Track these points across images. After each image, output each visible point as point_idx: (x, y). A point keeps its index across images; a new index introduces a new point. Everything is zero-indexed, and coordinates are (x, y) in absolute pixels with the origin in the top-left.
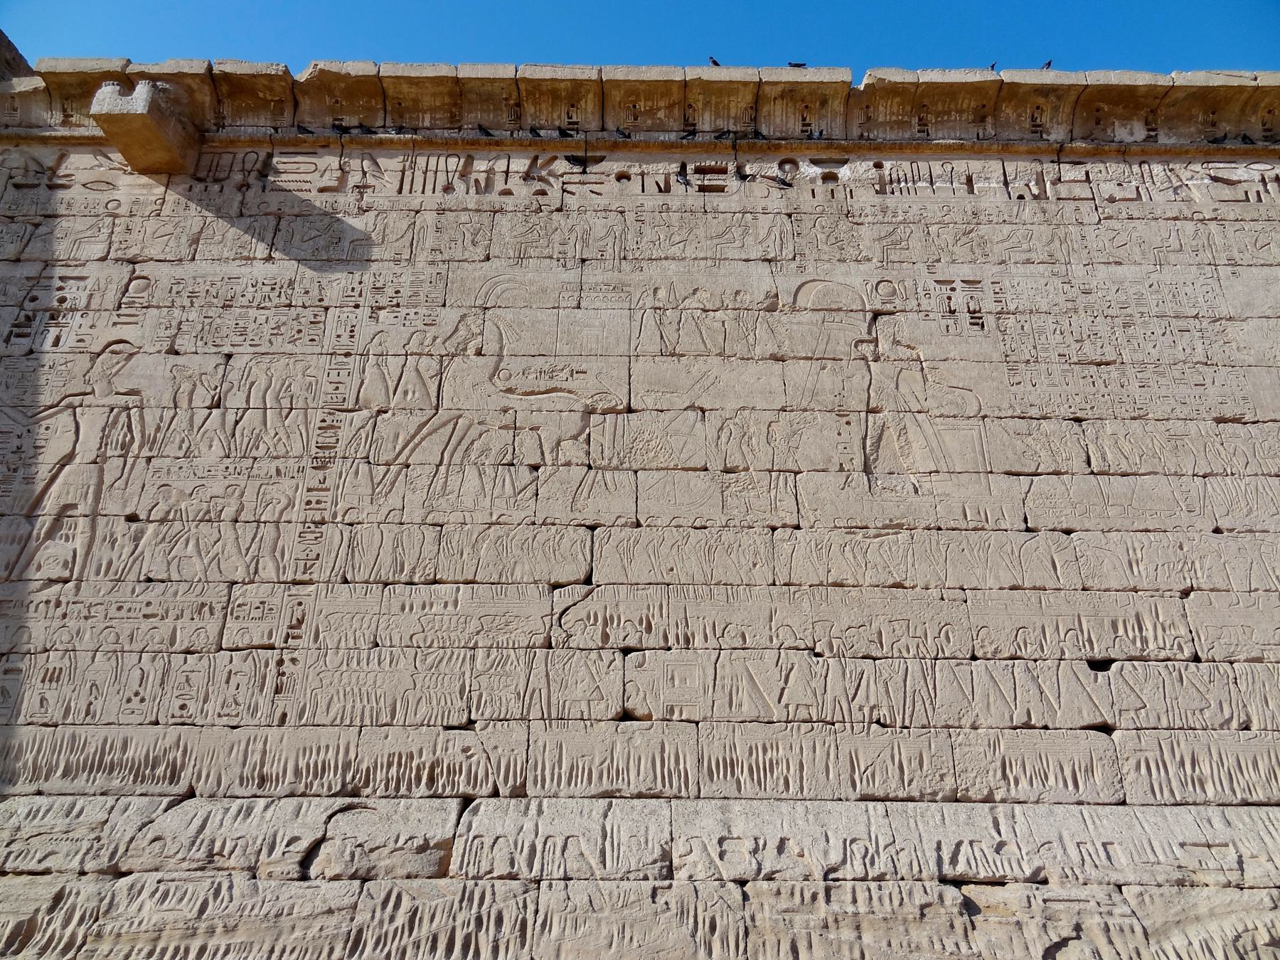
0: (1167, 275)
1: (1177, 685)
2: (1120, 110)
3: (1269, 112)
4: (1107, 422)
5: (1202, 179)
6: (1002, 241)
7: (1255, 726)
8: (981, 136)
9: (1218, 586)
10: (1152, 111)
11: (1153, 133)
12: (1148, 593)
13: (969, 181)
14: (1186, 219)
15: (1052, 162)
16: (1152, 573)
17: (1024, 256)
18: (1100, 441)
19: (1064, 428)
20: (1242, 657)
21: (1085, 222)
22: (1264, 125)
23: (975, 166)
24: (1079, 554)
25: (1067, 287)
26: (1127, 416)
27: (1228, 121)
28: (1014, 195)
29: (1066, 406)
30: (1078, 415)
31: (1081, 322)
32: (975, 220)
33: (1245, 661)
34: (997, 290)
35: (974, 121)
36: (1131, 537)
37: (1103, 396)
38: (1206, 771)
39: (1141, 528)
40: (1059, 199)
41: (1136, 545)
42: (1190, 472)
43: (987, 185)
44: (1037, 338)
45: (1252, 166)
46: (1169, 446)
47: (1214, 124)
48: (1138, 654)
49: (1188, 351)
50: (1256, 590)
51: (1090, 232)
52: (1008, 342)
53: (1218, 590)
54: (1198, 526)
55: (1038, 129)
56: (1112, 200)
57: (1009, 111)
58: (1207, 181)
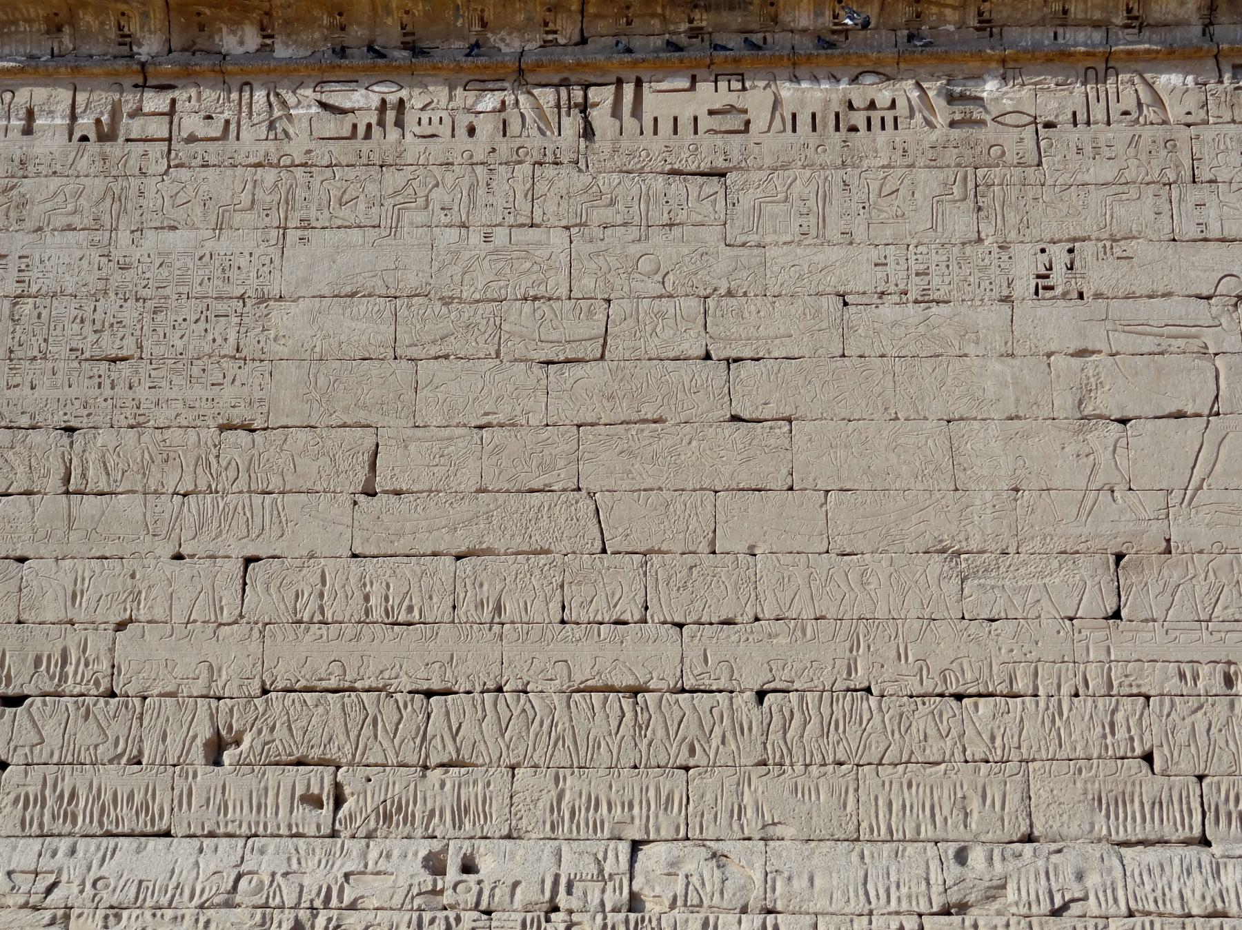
0: (224, 245)
1: (80, 720)
2: (225, 13)
3: (407, 12)
4: (100, 431)
5: (309, 106)
6: (46, 200)
7: (144, 761)
8: (56, 51)
9: (156, 618)
10: (266, 13)
11: (268, 41)
12: (82, 626)
13: (30, 114)
14: (271, 165)
15: (136, 86)
16: (94, 604)
17: (65, 221)
18: (87, 454)
19: (51, 441)
20: (156, 692)
21: (150, 172)
22: (403, 28)
23: (40, 94)
24: (24, 584)
25: (104, 260)
26: (125, 423)
27: (360, 24)
28: (77, 136)
29: (61, 413)
30: (71, 424)
31: (110, 304)
32: (21, 173)
33: (157, 696)
34: (23, 267)
35: (48, 32)
36: (85, 565)
37: (105, 400)
38: (82, 804)
39: (98, 554)
40: (128, 140)
41: (87, 575)
42: (171, 491)
43: (49, 122)
44: (52, 328)
45: (375, 88)
46: (158, 460)
47: (343, 28)
48: (52, 690)
49: (219, 341)
50: (195, 621)
51: (151, 184)
52: (17, 335)
53: (156, 622)
54: (158, 552)
55: (126, 39)
56: (192, 139)
57: (88, 18)
58: (315, 109)
